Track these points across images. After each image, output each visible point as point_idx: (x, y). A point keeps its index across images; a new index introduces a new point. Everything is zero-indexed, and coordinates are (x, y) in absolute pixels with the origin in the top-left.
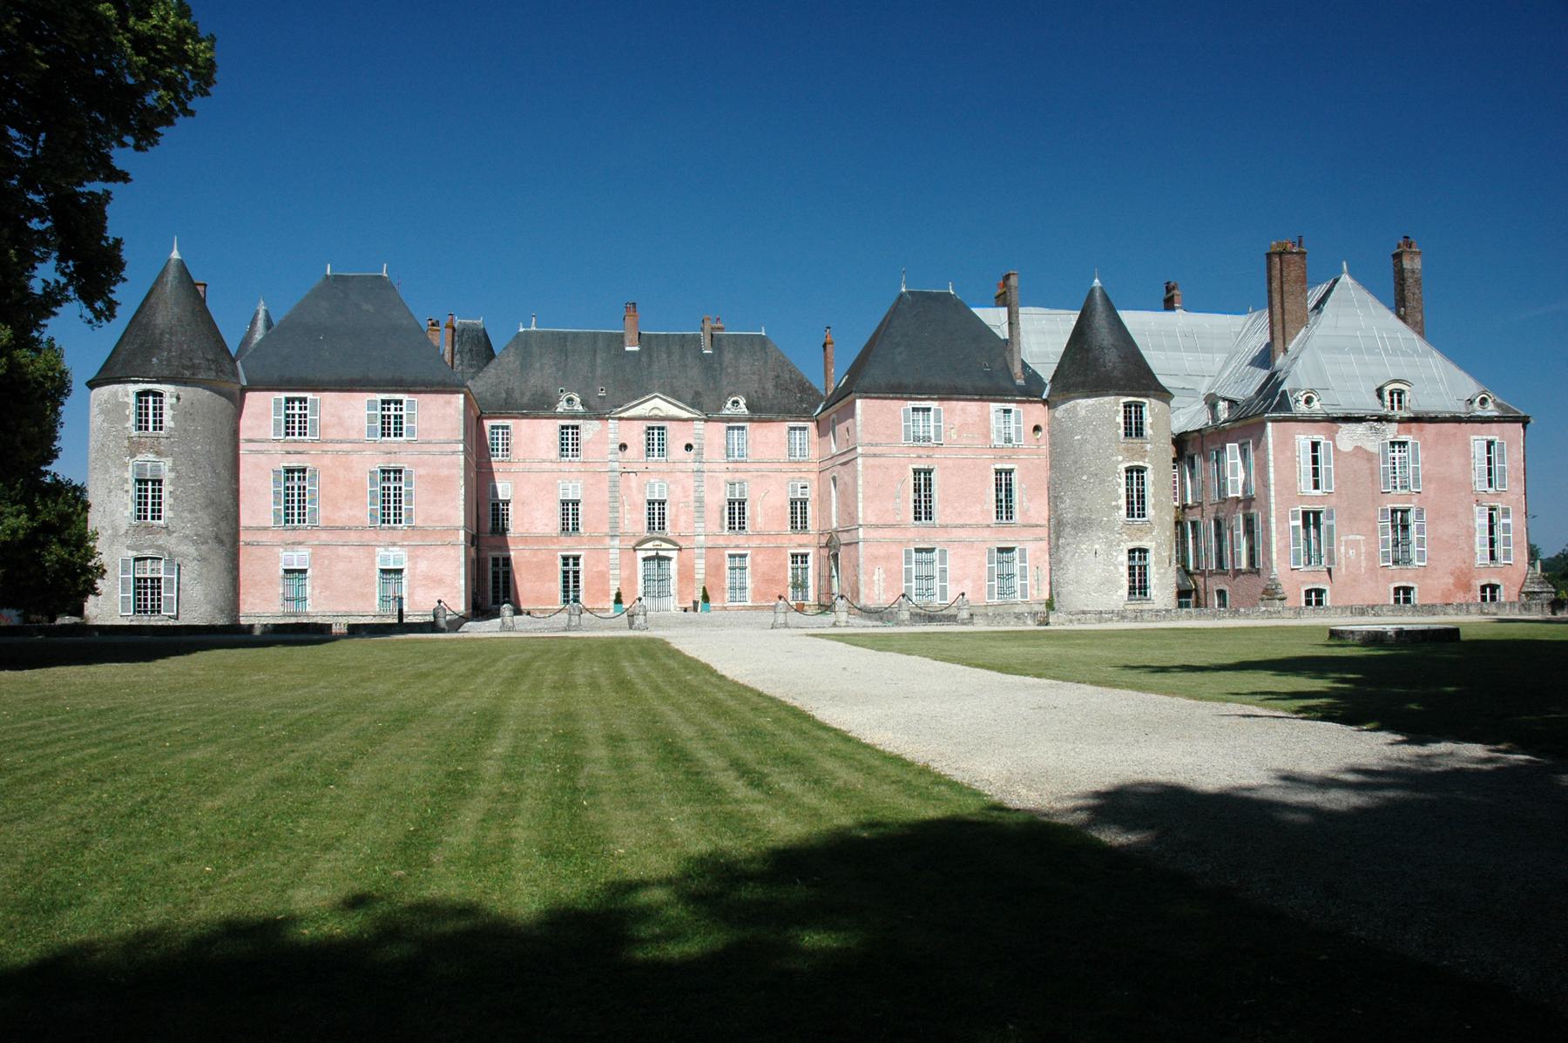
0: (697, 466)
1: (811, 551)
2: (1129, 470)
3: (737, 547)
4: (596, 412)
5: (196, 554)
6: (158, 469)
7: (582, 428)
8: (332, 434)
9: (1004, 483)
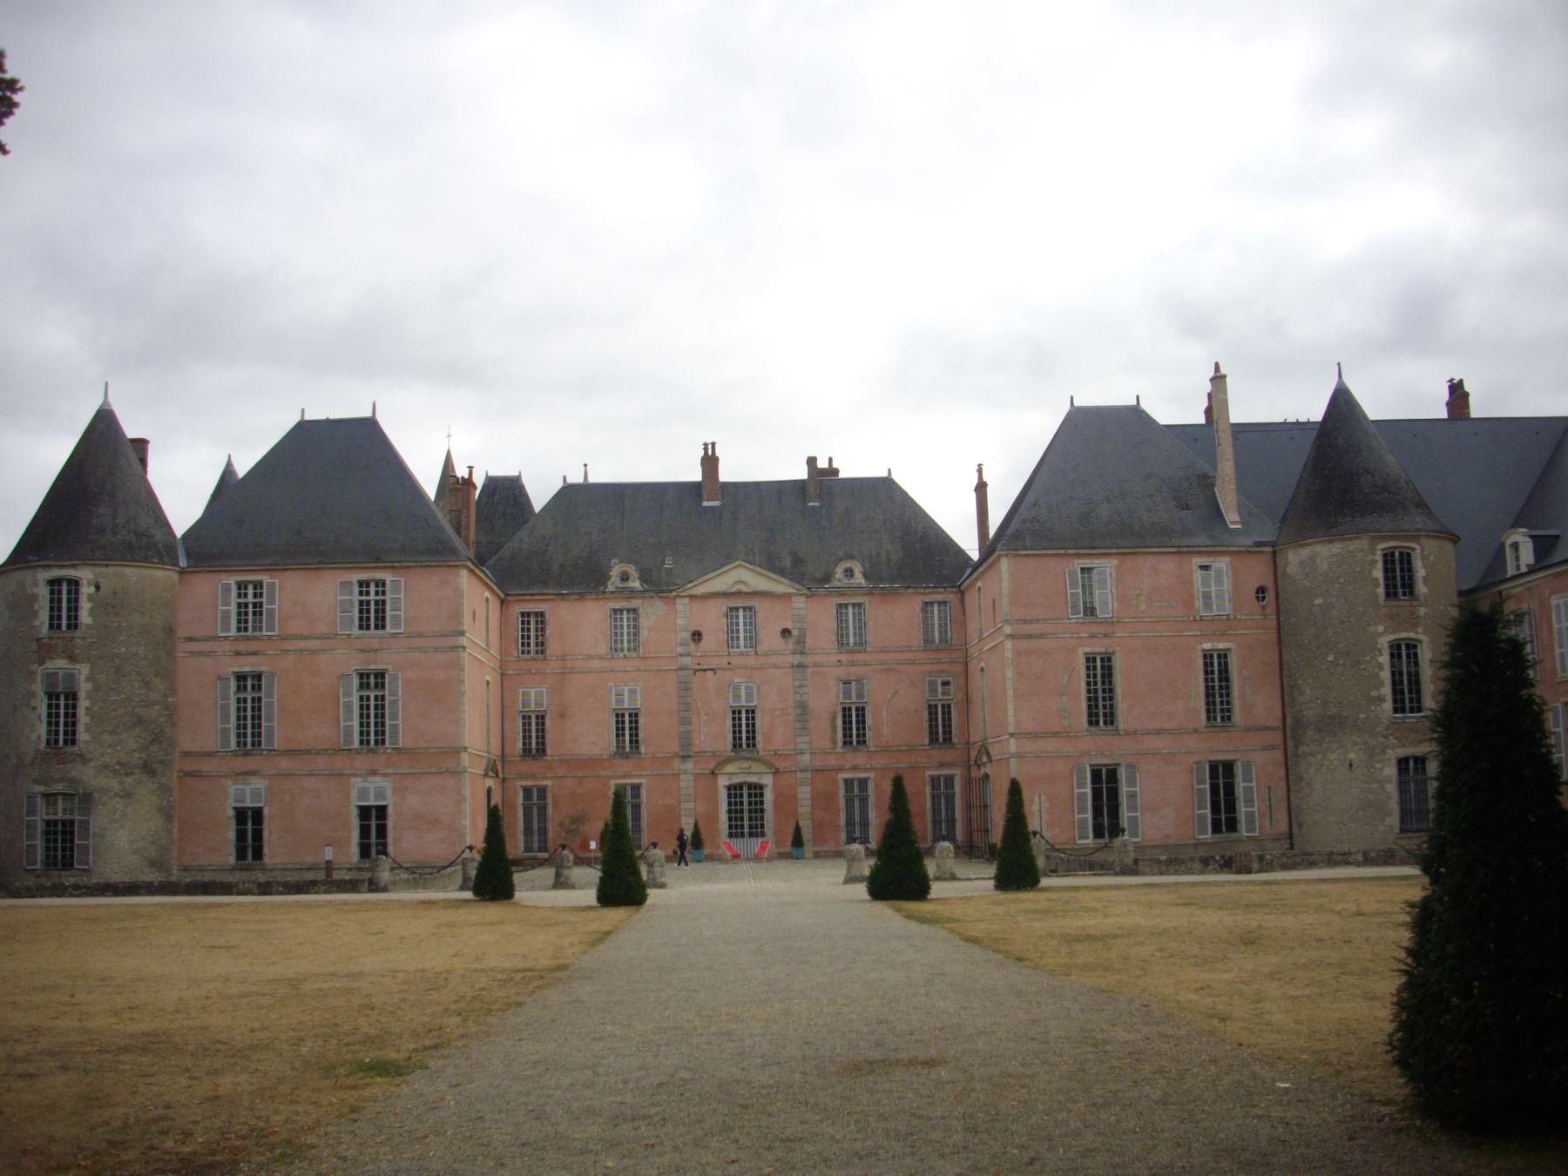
0: (797, 659)
1: (958, 773)
2: (1395, 650)
3: (855, 768)
4: (658, 586)
5: (118, 788)
6: (71, 677)
7: (642, 613)
8: (297, 627)
9: (1217, 672)
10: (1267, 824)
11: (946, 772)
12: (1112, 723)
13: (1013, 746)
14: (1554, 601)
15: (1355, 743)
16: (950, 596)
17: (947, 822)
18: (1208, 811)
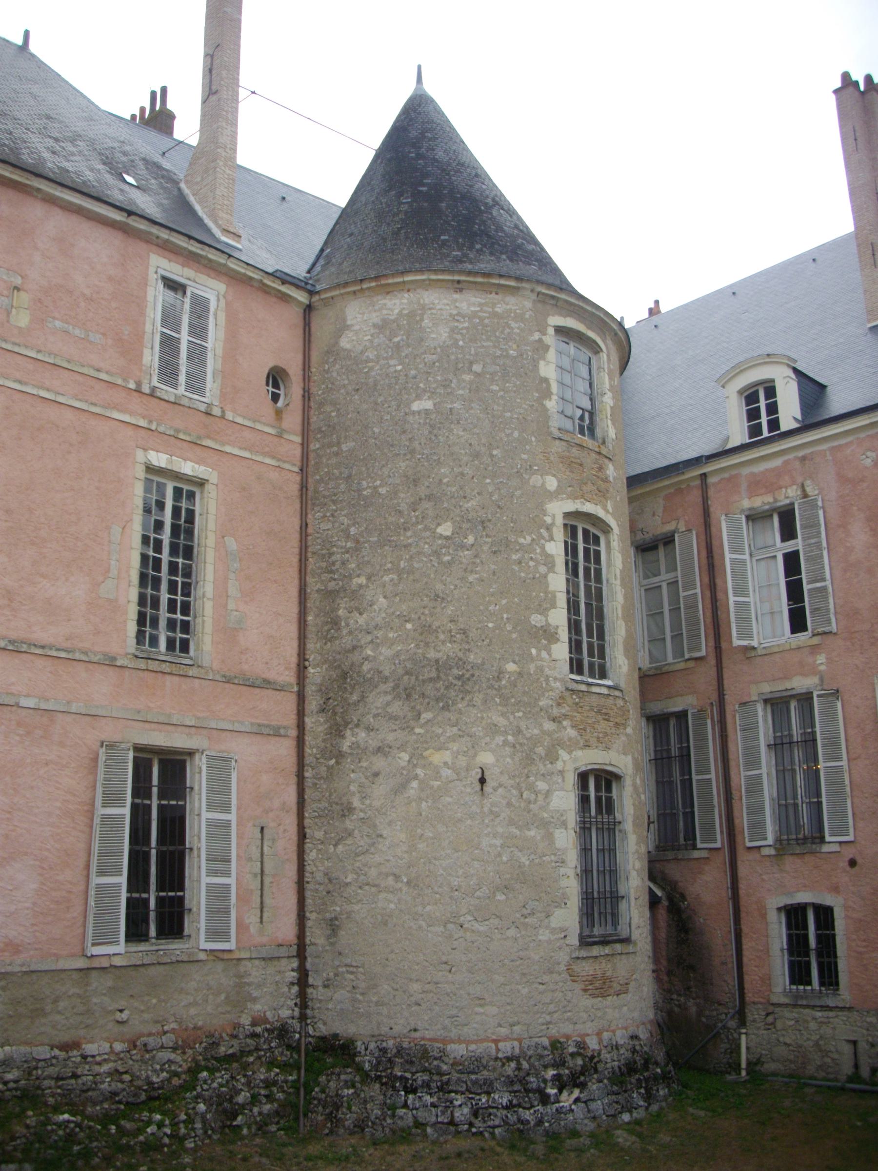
10: (252, 919)
15: (493, 730)
18: (123, 879)
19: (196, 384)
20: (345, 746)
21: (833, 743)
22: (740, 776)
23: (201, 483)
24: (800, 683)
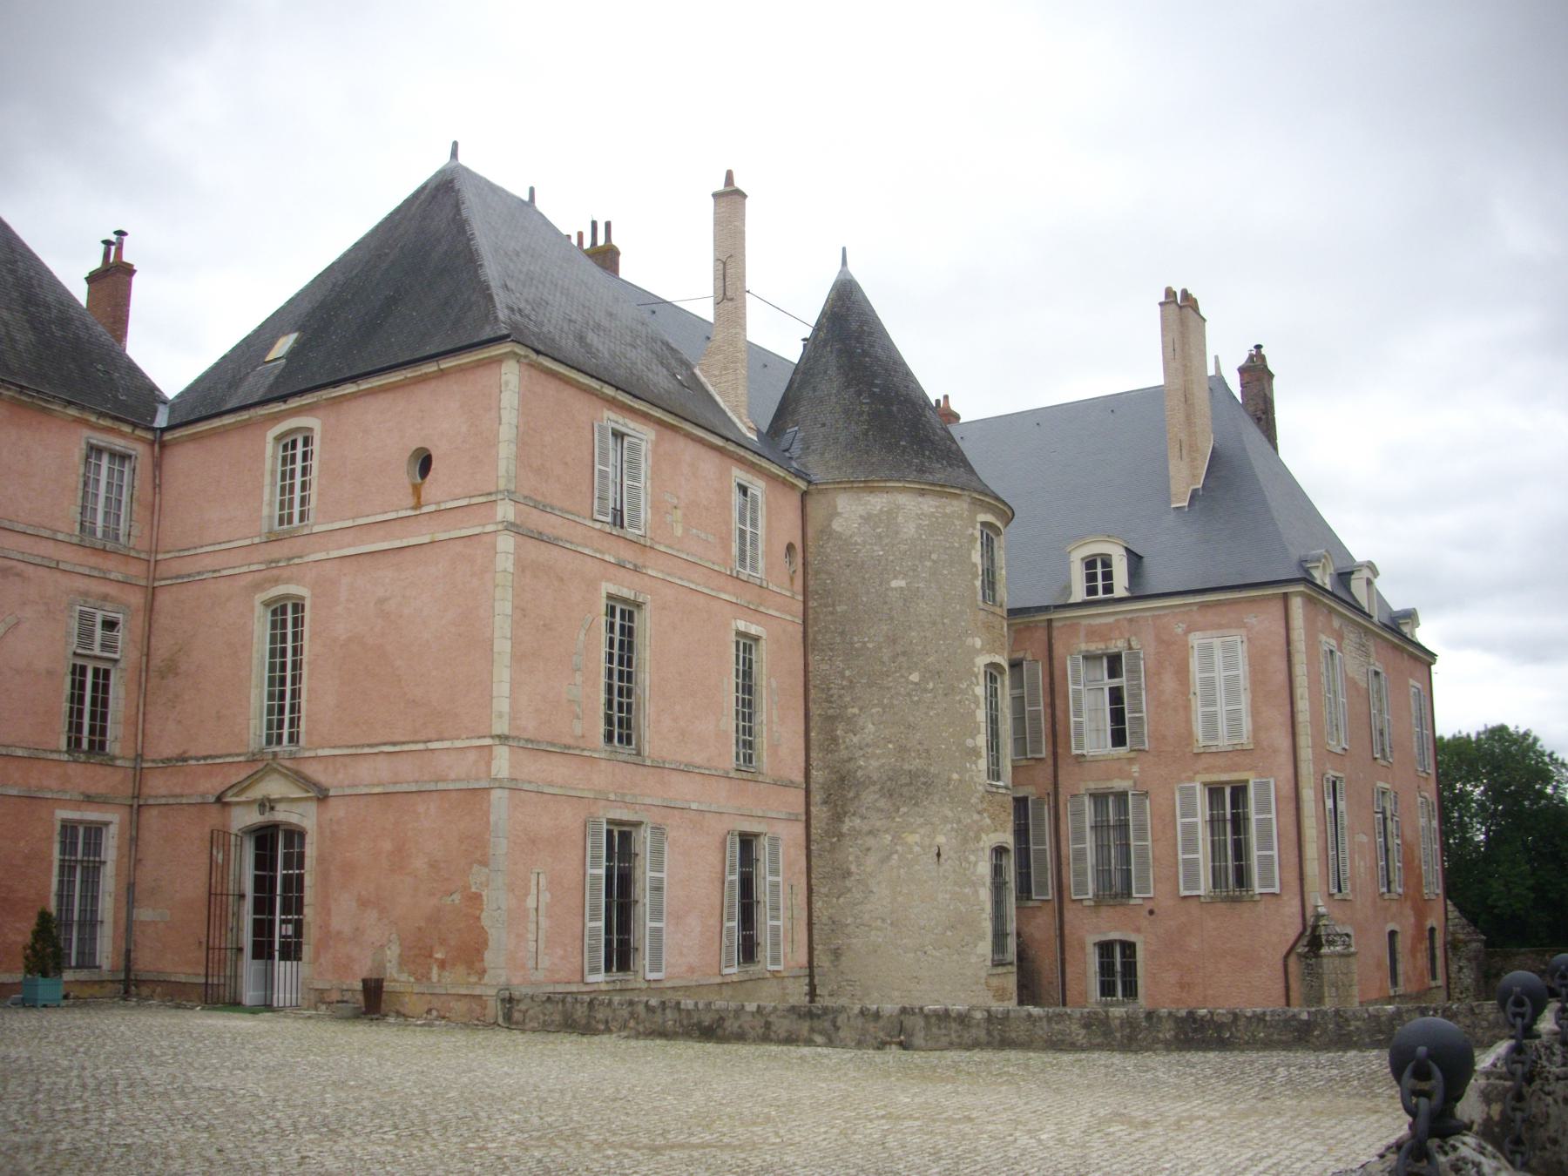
1: (114, 819)
11: (92, 815)
12: (626, 739)
13: (502, 763)
14: (1196, 639)
15: (945, 819)
16: (140, 450)
17: (81, 924)
19: (754, 568)
20: (845, 829)
21: (1141, 829)
22: (1069, 848)
23: (757, 639)
24: (1119, 784)
